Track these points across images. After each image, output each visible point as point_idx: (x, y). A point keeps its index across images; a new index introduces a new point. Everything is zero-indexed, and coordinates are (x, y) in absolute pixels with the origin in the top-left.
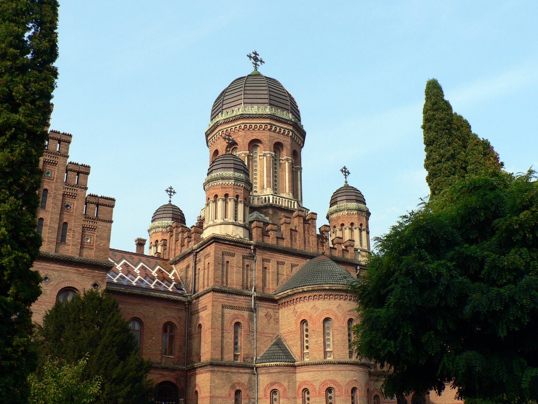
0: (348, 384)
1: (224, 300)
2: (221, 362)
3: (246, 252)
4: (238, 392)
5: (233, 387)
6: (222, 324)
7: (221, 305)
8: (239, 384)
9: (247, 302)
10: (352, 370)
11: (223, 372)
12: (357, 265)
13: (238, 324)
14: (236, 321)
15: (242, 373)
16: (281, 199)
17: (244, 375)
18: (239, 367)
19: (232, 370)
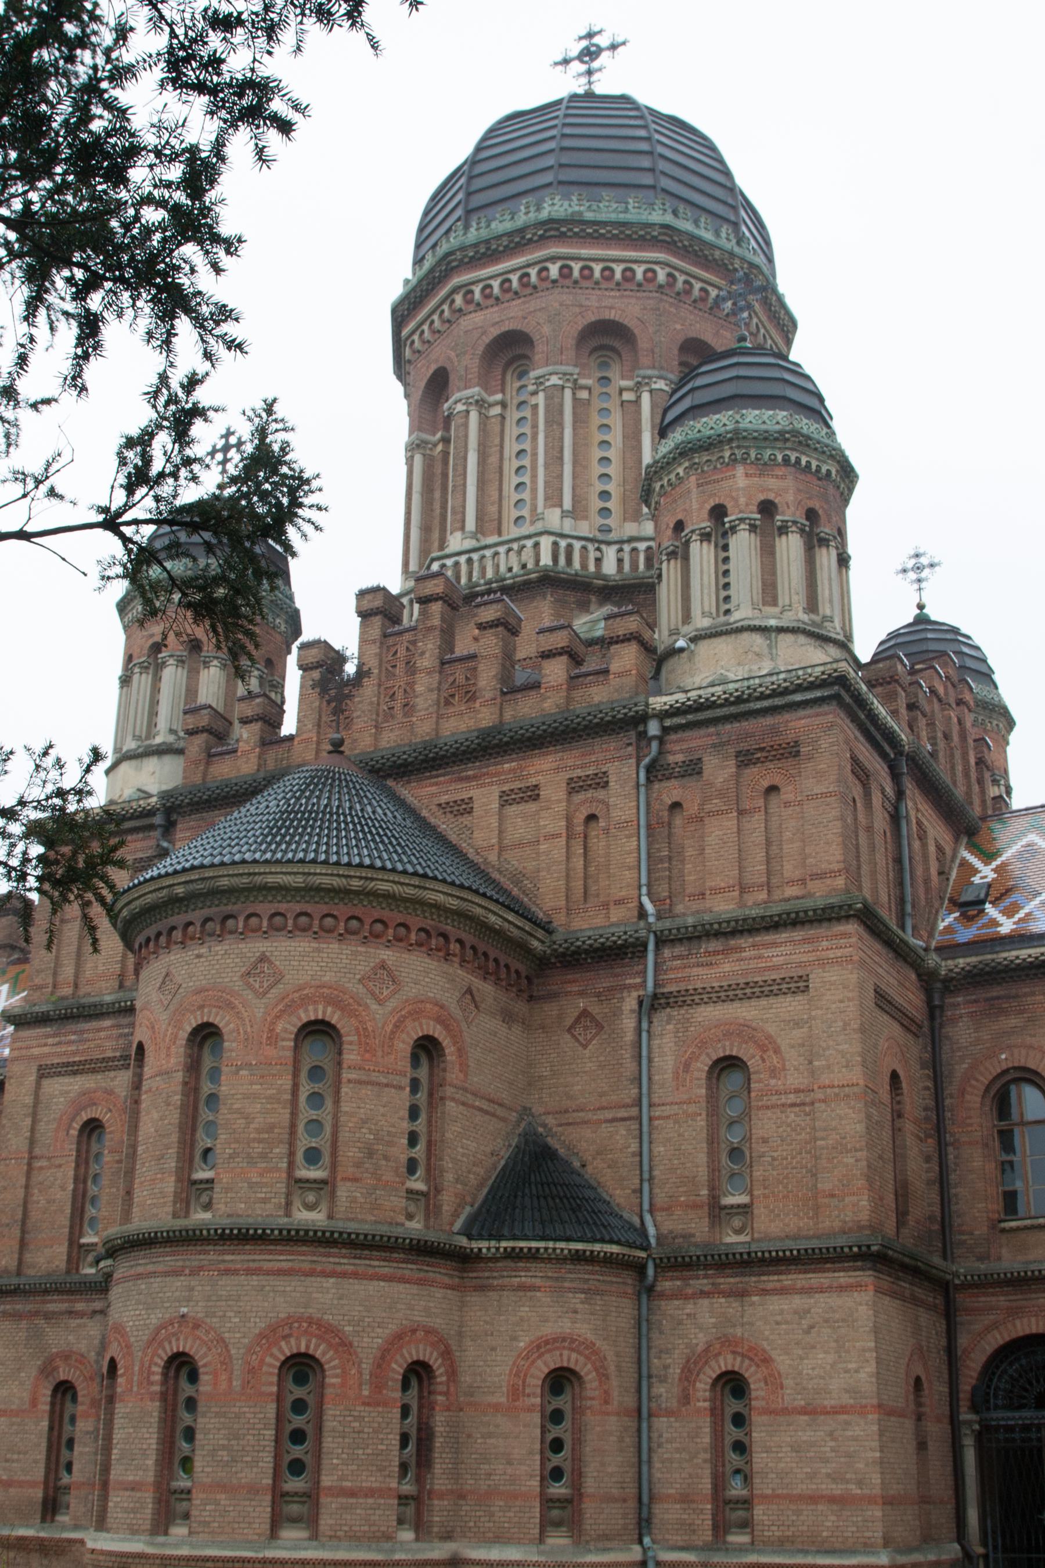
0: (153, 1340)
1: (46, 1050)
2: (23, 1280)
3: (145, 844)
4: (64, 1390)
5: (47, 1370)
6: (32, 1142)
7: (34, 1069)
8: (66, 1356)
9: (121, 1035)
10: (176, 1273)
11: (17, 1316)
12: (643, 718)
13: (93, 1127)
14: (85, 1116)
15: (80, 1314)
16: (475, 556)
17: (90, 1323)
18: (70, 1292)
19: (51, 1307)
